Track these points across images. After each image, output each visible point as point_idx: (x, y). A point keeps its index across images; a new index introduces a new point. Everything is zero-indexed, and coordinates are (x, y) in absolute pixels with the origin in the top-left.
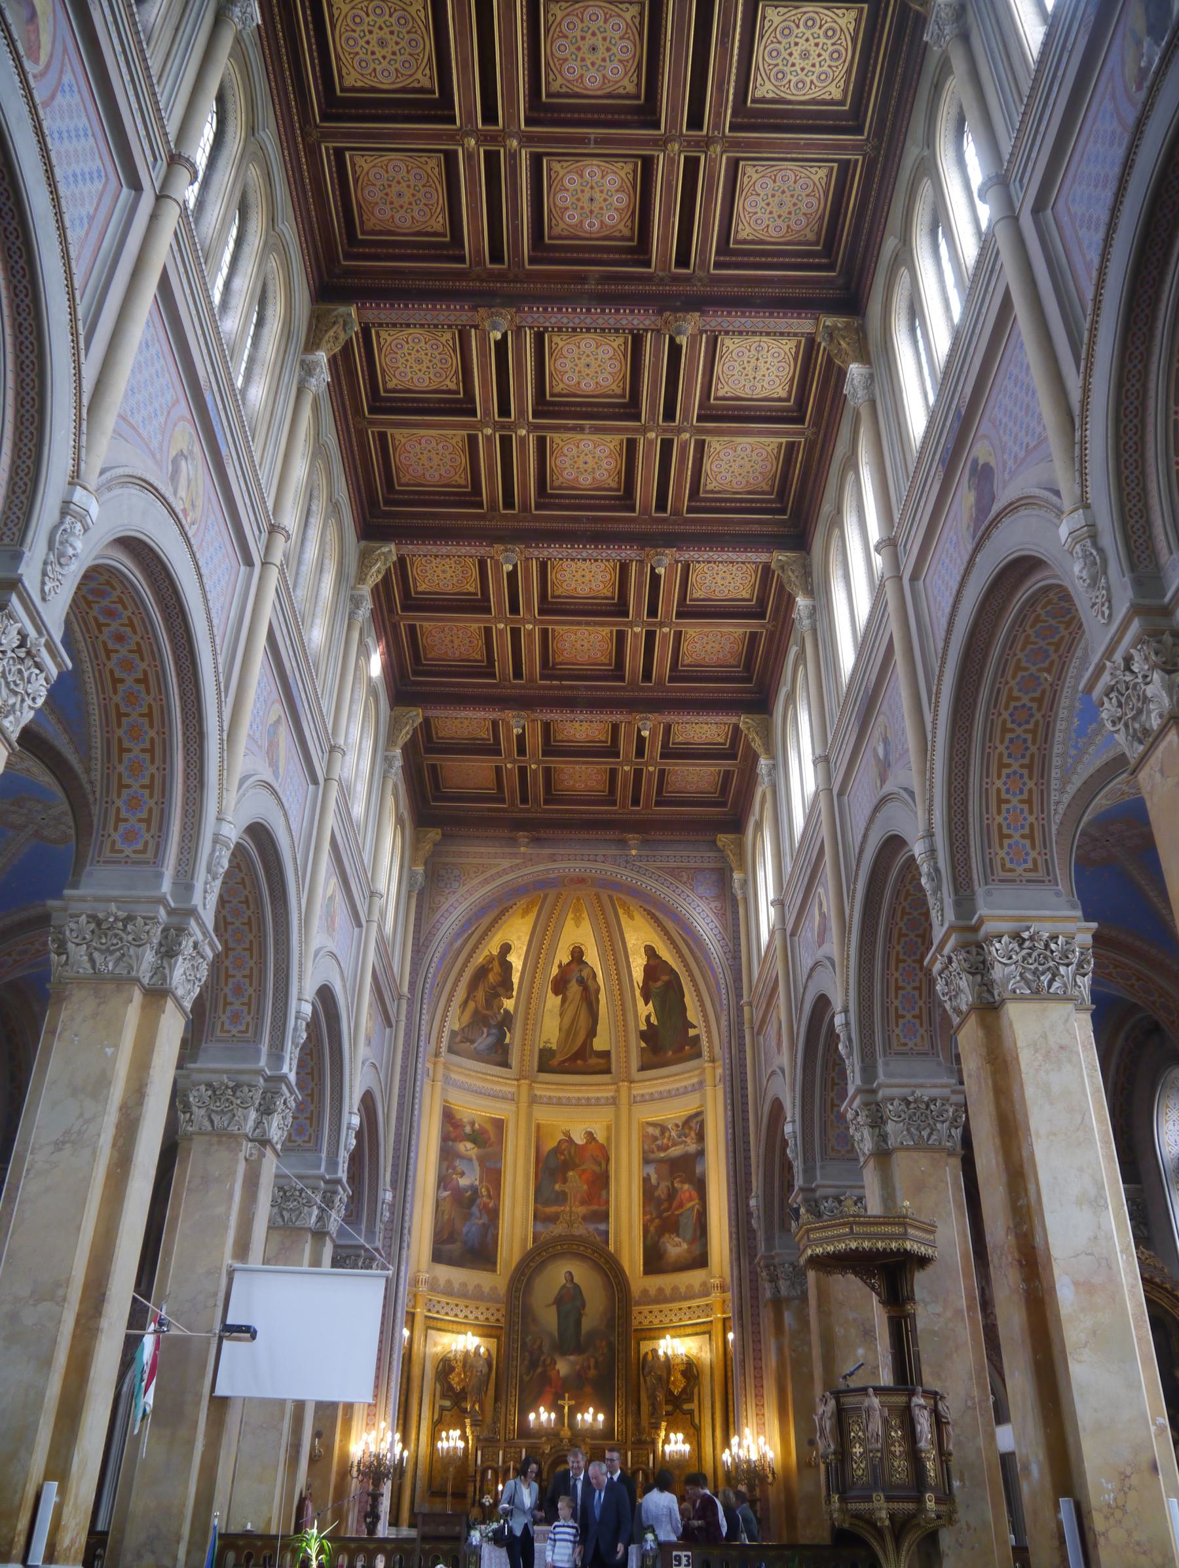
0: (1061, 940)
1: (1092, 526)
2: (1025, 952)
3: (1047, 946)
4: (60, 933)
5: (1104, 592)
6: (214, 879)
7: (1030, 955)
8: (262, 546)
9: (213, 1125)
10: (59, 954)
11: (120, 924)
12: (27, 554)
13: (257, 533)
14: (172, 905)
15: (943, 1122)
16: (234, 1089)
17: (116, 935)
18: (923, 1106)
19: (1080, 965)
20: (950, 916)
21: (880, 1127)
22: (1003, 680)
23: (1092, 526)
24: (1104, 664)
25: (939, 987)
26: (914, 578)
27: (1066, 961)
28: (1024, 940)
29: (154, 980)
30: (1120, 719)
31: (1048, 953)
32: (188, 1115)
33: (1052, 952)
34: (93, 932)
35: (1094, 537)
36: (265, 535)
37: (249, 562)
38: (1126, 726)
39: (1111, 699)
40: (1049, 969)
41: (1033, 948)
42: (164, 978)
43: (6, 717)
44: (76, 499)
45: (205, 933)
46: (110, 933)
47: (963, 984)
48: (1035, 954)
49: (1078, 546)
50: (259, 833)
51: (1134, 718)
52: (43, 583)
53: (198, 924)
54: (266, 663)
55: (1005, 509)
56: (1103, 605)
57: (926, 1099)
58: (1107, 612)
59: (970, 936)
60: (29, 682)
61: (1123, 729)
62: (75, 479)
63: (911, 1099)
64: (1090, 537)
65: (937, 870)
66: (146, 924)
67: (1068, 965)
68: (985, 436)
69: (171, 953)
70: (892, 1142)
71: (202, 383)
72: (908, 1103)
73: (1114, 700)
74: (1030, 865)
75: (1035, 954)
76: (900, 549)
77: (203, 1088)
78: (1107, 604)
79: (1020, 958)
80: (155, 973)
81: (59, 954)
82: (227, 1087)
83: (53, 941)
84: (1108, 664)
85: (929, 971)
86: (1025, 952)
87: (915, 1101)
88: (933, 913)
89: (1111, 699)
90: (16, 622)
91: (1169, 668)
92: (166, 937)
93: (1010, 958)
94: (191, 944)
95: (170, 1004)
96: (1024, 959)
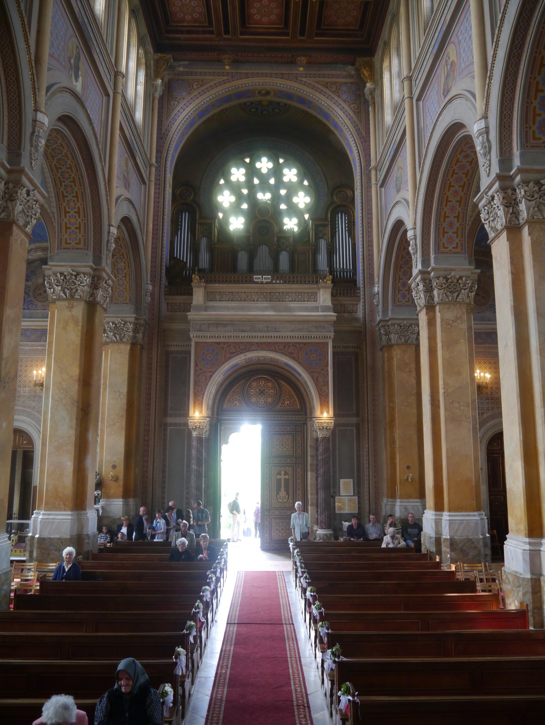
0: (464, 279)
1: (487, 128)
2: (448, 283)
3: (458, 281)
4: (49, 279)
5: (488, 162)
6: (110, 252)
7: (450, 285)
8: (112, 84)
9: (116, 339)
10: (50, 289)
11: (74, 277)
12: (23, 153)
13: (109, 77)
14: (94, 267)
15: (414, 334)
16: (124, 325)
17: (73, 282)
18: (407, 327)
19: (471, 288)
20: (420, 267)
21: (389, 335)
22: (447, 179)
23: (487, 128)
24: (483, 196)
25: (414, 293)
26: (418, 100)
27: (465, 288)
28: (449, 279)
29: (91, 299)
30: (487, 219)
31: (458, 284)
32: (106, 335)
33: (460, 284)
34: (63, 280)
35: (487, 133)
36: (113, 77)
37: (108, 95)
38: (489, 222)
39: (485, 210)
40: (457, 291)
41: (452, 282)
42: (95, 299)
43: (26, 227)
44: (38, 119)
45: (109, 276)
46: (71, 281)
47: (422, 296)
48: (452, 285)
49: (480, 137)
50: (126, 221)
51: (493, 221)
52: (31, 163)
53: (105, 273)
54: (120, 141)
55: (454, 96)
56: (487, 167)
57: (408, 325)
58: (488, 172)
59: (426, 276)
60: (33, 208)
61: (488, 224)
62: (36, 110)
63: (402, 325)
64: (485, 133)
65: (416, 245)
66: (85, 277)
67: (465, 289)
68: (453, 43)
69: (97, 287)
70: (393, 341)
71: (78, 16)
72: (401, 327)
73: (486, 211)
74: (455, 245)
75: (452, 285)
76: (413, 83)
77: (111, 324)
78: (488, 168)
79: (446, 286)
80: (91, 296)
81: (50, 289)
82: (121, 323)
83: (47, 283)
84: (485, 196)
85: (410, 287)
86: (448, 283)
87: (404, 326)
88: (413, 262)
89: (485, 210)
90: (24, 187)
91: (508, 205)
92: (94, 281)
93: (442, 286)
94: (104, 282)
95: (98, 307)
96: (447, 287)
